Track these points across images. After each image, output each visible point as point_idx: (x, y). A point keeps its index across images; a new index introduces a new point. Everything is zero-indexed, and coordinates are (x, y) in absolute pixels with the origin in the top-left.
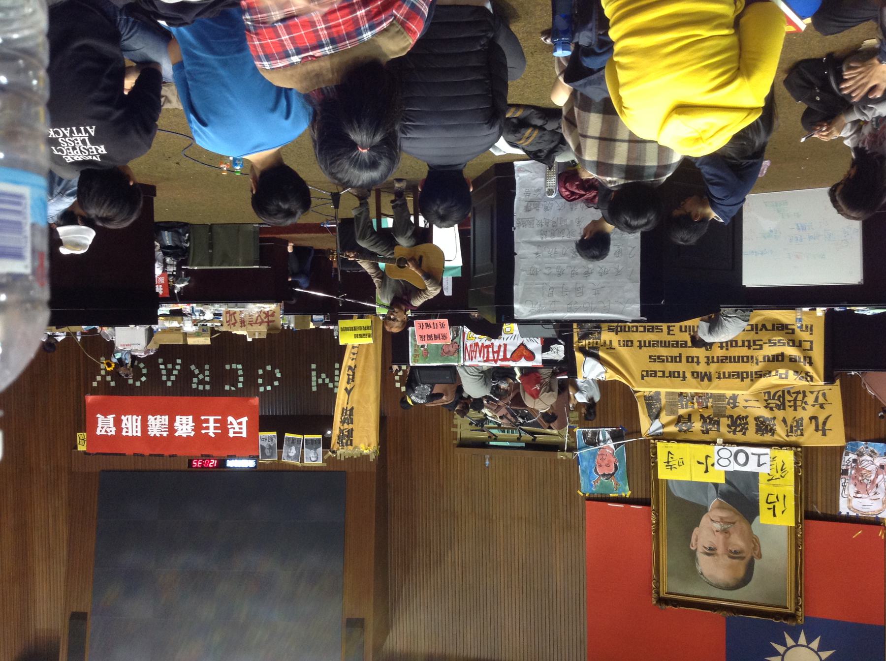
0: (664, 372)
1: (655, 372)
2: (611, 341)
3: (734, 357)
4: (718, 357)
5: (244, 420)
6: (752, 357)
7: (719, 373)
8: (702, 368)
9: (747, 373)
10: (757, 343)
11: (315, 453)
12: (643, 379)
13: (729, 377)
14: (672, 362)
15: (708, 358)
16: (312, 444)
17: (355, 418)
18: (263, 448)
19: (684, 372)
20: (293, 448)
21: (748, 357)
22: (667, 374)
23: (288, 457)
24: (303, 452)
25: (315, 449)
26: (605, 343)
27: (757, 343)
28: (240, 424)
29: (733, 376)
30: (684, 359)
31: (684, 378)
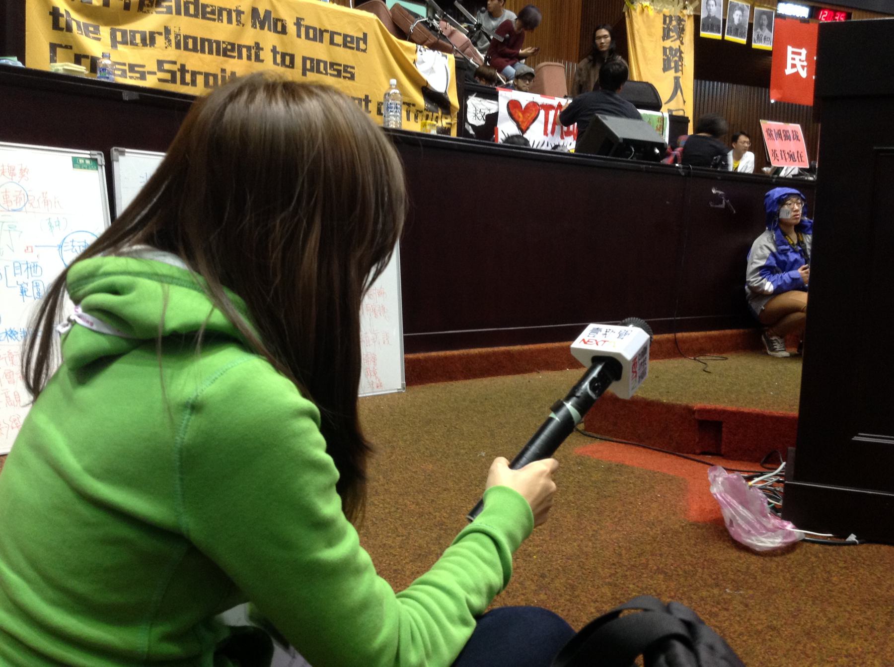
0: (332, 42)
1: (345, 46)
2: (408, 119)
3: (211, 52)
4: (240, 57)
5: (789, 71)
6: (178, 46)
7: (239, 22)
8: (269, 39)
9: (187, 13)
10: (168, 76)
11: (709, 11)
12: (365, 35)
13: (221, 10)
14: (319, 61)
15: (258, 59)
16: (712, 25)
17: (661, 56)
18: (769, 26)
19: (299, 36)
20: (736, 22)
21: (186, 48)
22: (327, 36)
23: (742, 10)
24: (725, 13)
25: (709, 17)
26: (416, 117)
27: (168, 76)
28: (794, 66)
29: (213, 12)
30: (298, 62)
31: (298, 23)
